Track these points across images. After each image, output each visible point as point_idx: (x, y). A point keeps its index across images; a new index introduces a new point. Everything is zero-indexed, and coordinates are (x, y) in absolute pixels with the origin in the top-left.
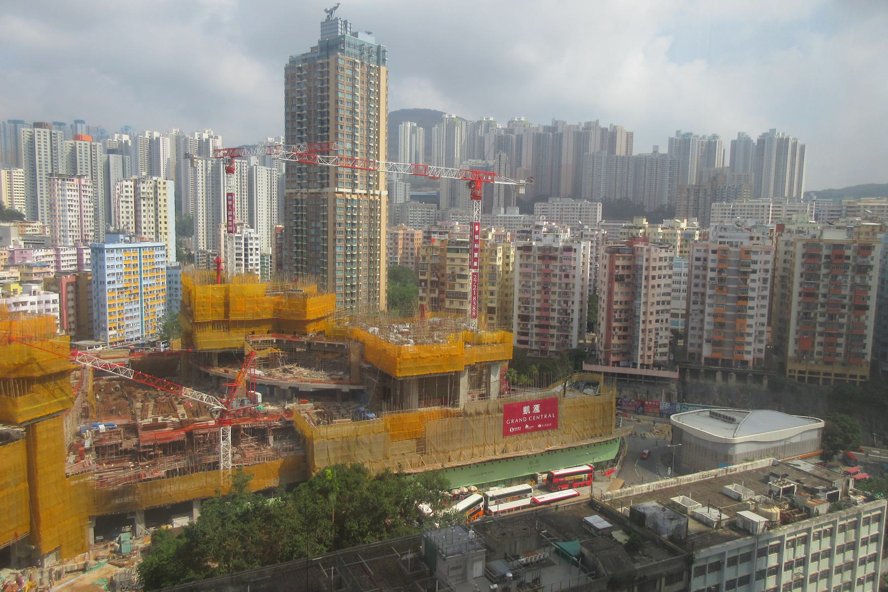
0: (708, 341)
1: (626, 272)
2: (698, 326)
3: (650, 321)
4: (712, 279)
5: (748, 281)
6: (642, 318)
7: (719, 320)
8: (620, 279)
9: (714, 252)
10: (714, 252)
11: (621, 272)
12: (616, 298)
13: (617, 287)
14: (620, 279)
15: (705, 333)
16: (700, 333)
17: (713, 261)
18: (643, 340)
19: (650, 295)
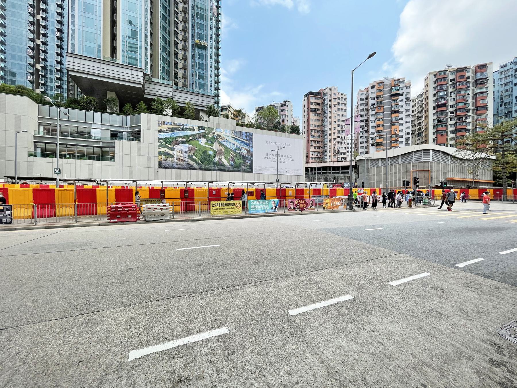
0: (372, 145)
1: (318, 107)
2: (364, 140)
3: (334, 133)
4: (372, 104)
5: (398, 101)
6: (329, 132)
7: (380, 128)
8: (314, 111)
9: (373, 87)
10: (373, 87)
11: (312, 106)
12: (311, 122)
13: (312, 115)
14: (314, 111)
15: (370, 139)
16: (366, 145)
17: (373, 93)
18: (330, 146)
19: (333, 117)
